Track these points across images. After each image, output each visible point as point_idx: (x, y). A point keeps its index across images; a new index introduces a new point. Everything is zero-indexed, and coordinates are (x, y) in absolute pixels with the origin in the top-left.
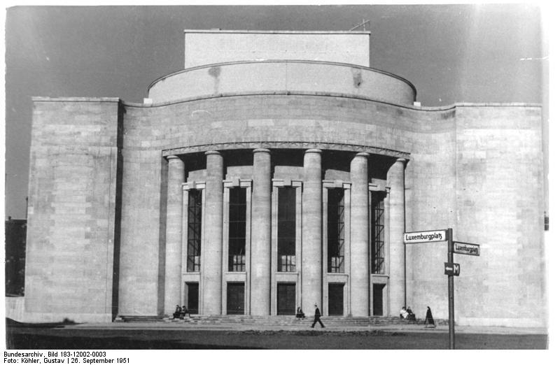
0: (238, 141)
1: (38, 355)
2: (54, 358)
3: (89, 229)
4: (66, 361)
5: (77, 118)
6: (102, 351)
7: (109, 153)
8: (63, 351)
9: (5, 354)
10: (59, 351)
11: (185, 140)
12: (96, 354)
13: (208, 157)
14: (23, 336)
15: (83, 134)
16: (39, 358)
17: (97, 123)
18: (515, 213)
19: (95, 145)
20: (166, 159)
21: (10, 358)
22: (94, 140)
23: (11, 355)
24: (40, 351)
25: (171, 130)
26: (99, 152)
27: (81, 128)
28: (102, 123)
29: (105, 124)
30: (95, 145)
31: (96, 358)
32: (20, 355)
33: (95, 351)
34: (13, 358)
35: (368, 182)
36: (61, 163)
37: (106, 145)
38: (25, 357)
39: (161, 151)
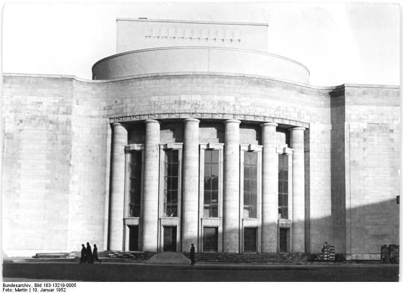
0: (173, 112)
1: (27, 286)
3: (48, 181)
4: (29, 290)
6: (74, 283)
7: (65, 120)
8: (46, 283)
9: (4, 285)
10: (43, 283)
16: (28, 288)
17: (55, 95)
18: (389, 172)
20: (113, 126)
21: (7, 288)
22: (54, 109)
24: (29, 283)
26: (57, 119)
28: (60, 96)
29: (62, 96)
31: (48, 288)
32: (14, 286)
33: (69, 283)
34: (10, 288)
36: (26, 127)
37: (64, 113)
38: (18, 287)
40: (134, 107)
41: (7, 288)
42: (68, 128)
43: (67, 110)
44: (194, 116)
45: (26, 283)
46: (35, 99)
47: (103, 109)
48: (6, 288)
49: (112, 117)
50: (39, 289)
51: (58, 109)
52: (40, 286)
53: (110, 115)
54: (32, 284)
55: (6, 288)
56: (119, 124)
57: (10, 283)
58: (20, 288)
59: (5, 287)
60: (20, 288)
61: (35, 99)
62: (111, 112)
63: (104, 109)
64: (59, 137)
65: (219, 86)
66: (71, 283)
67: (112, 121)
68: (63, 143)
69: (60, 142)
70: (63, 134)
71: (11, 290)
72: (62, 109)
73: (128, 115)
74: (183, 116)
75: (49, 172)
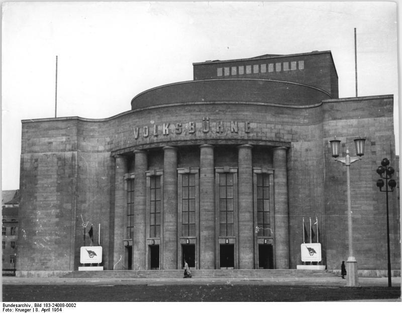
4: (32, 311)
5: (50, 132)
13: (136, 155)
14: (13, 294)
15: (54, 143)
17: (63, 135)
19: (62, 151)
20: (113, 158)
22: (61, 147)
29: (69, 136)
35: (253, 167)
39: (110, 153)
41: (7, 308)
42: (73, 163)
43: (72, 147)
44: (169, 144)
45: (26, 303)
47: (107, 143)
48: (6, 308)
49: (113, 150)
50: (40, 309)
51: (66, 147)
52: (40, 306)
54: (32, 304)
55: (6, 308)
56: (118, 156)
57: (10, 303)
58: (19, 308)
60: (19, 308)
61: (47, 140)
62: (113, 146)
63: (108, 144)
64: (66, 171)
65: (191, 115)
66: (71, 303)
69: (67, 175)
71: (11, 310)
72: (68, 147)
73: (122, 148)
74: (161, 145)
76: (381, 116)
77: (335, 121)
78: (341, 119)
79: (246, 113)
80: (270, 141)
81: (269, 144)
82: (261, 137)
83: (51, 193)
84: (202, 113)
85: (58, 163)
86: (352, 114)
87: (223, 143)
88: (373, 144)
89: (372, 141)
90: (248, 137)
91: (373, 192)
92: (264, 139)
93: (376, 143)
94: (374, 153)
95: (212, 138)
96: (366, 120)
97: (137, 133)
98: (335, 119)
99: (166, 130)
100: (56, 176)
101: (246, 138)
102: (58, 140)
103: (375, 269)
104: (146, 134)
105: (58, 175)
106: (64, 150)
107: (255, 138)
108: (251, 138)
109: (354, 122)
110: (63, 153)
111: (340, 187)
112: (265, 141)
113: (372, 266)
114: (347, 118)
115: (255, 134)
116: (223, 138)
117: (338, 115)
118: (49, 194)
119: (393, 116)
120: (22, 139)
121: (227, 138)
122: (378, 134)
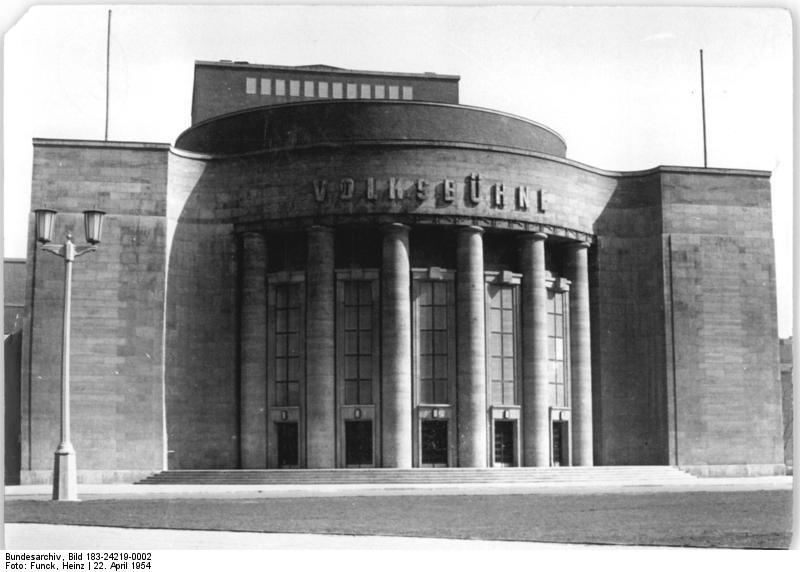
1: (54, 558)
2: (78, 562)
3: (123, 342)
9: (8, 556)
11: (275, 208)
12: (137, 556)
17: (135, 180)
20: (238, 237)
21: (14, 562)
22: (131, 205)
23: (16, 557)
25: (249, 194)
27: (109, 188)
28: (143, 181)
29: (148, 182)
30: (131, 212)
32: (28, 557)
34: (19, 562)
37: (150, 213)
38: (35, 560)
40: (285, 203)
43: (157, 206)
46: (94, 187)
47: (221, 206)
53: (237, 218)
59: (10, 561)
61: (94, 187)
64: (142, 257)
67: (241, 229)
68: (150, 269)
69: (145, 267)
70: (150, 252)
72: (146, 206)
75: (124, 324)
76: (753, 205)
77: (681, 205)
78: (691, 203)
79: (541, 175)
80: (572, 230)
81: (572, 236)
82: (563, 221)
83: (104, 301)
84: (468, 165)
85: (121, 239)
86: (708, 196)
87: (504, 225)
88: (742, 251)
89: (741, 245)
90: (544, 219)
91: (744, 333)
92: (565, 225)
93: (747, 250)
94: (743, 266)
95: (485, 215)
96: (731, 210)
97: (323, 191)
98: (681, 201)
99: (396, 191)
100: (118, 267)
101: (541, 221)
102: (123, 190)
103: (745, 463)
104: (347, 194)
105: (122, 263)
106: (138, 212)
107: (554, 223)
108: (547, 223)
109: (712, 209)
110: (135, 218)
111: (691, 321)
112: (566, 229)
113: (740, 459)
114: (702, 201)
115: (554, 215)
116: (505, 217)
117: (687, 195)
118: (101, 304)
119: (770, 207)
120: (34, 179)
121: (512, 218)
122: (748, 235)
